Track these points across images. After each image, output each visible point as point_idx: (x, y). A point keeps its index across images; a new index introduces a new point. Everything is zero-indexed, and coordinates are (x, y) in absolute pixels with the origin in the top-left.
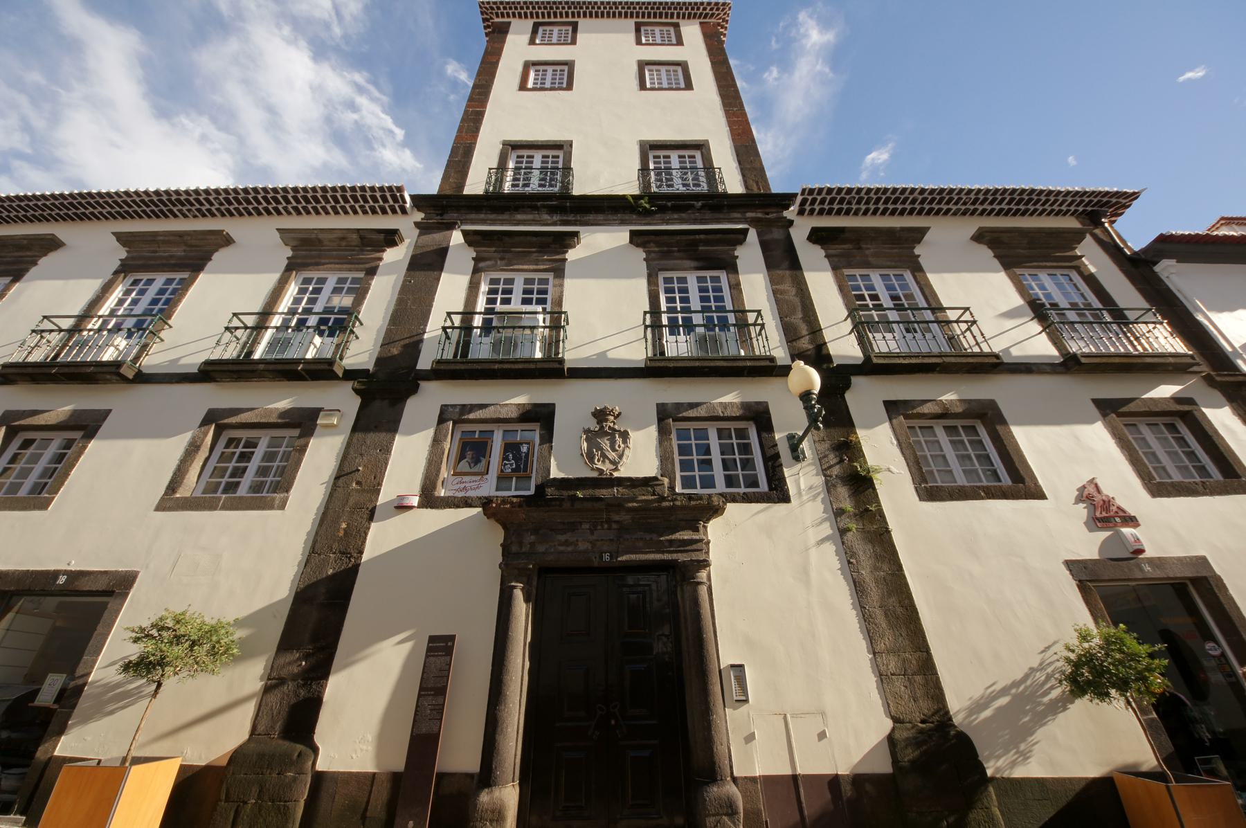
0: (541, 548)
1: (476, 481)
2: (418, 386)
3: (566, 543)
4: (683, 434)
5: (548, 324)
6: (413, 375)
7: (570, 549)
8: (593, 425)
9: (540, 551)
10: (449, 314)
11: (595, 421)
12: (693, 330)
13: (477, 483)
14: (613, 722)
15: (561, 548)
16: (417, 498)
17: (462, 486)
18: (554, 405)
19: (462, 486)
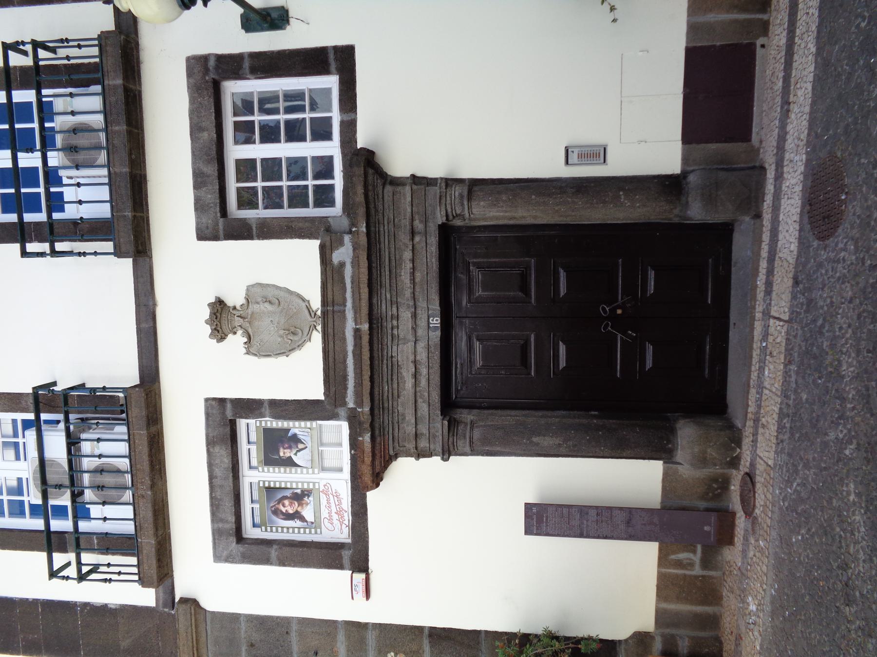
0: (423, 408)
1: (328, 501)
2: (184, 601)
3: (415, 376)
4: (247, 200)
5: (60, 417)
6: (166, 610)
7: (424, 371)
8: (236, 341)
9: (426, 410)
10: (53, 574)
11: (230, 336)
12: (56, 169)
13: (331, 496)
14: (619, 312)
15: (423, 382)
16: (355, 575)
17: (335, 517)
18: (207, 400)
19: (335, 517)
